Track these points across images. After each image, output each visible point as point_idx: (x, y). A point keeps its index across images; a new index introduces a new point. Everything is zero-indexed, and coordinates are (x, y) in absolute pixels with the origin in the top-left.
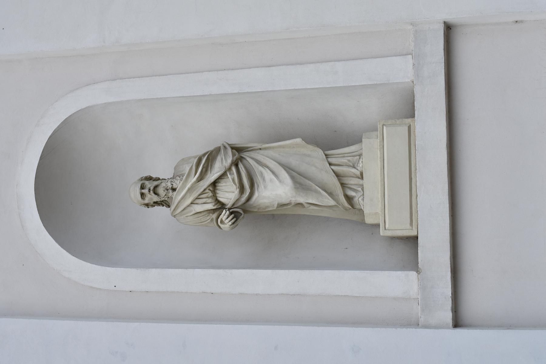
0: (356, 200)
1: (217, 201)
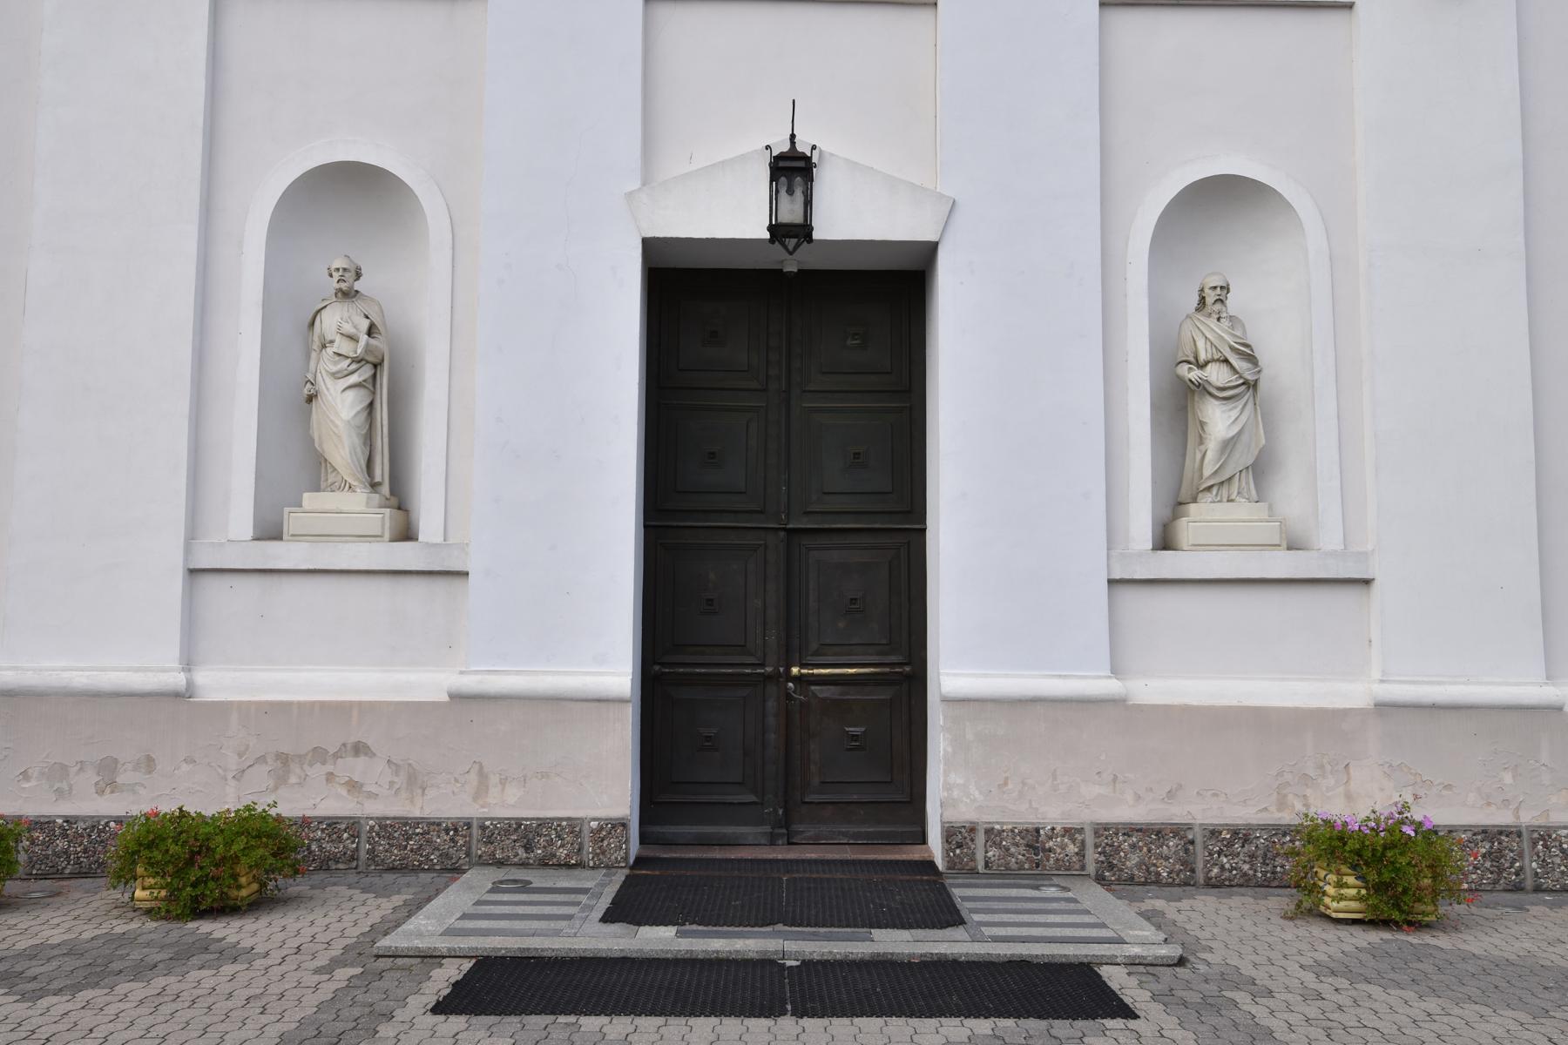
0: (1209, 495)
1: (1207, 363)
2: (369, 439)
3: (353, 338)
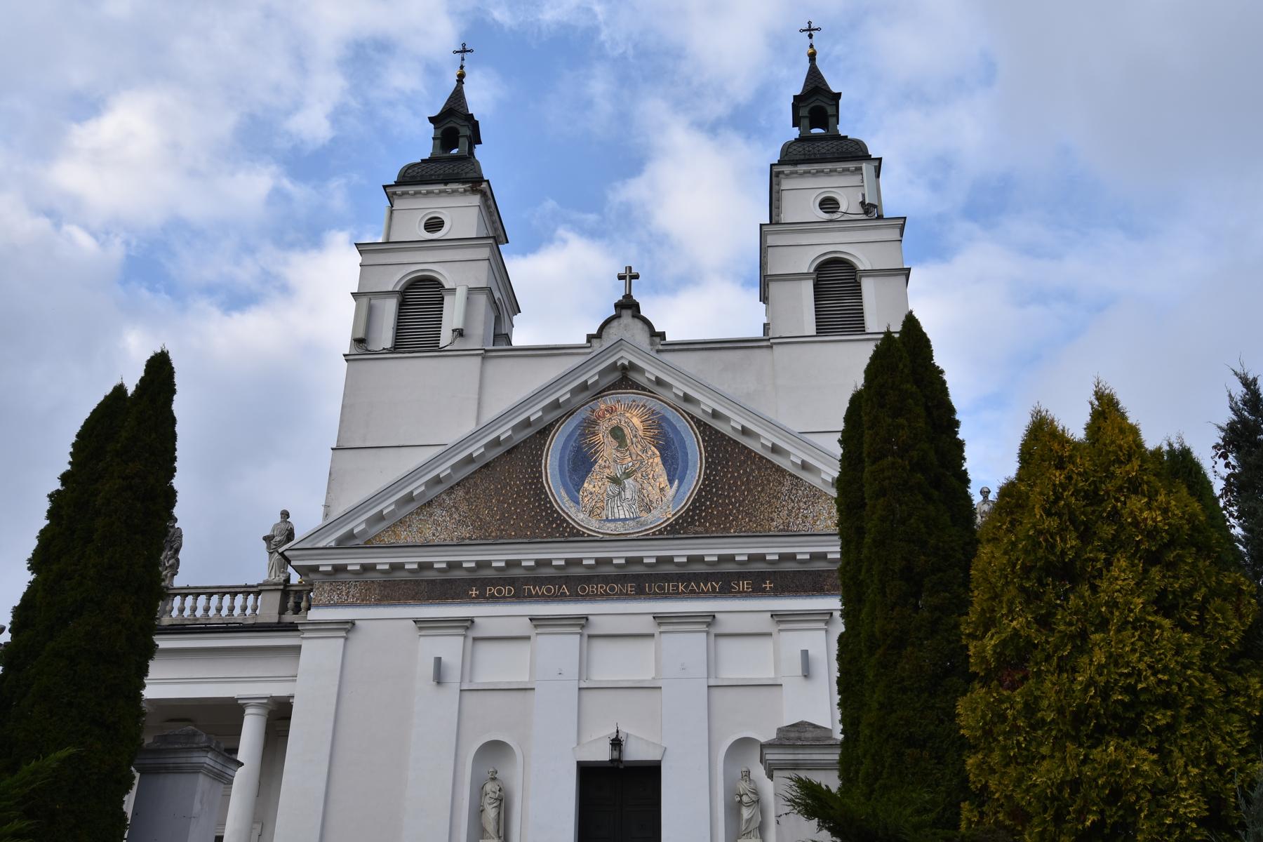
2: (498, 823)
3: (495, 792)
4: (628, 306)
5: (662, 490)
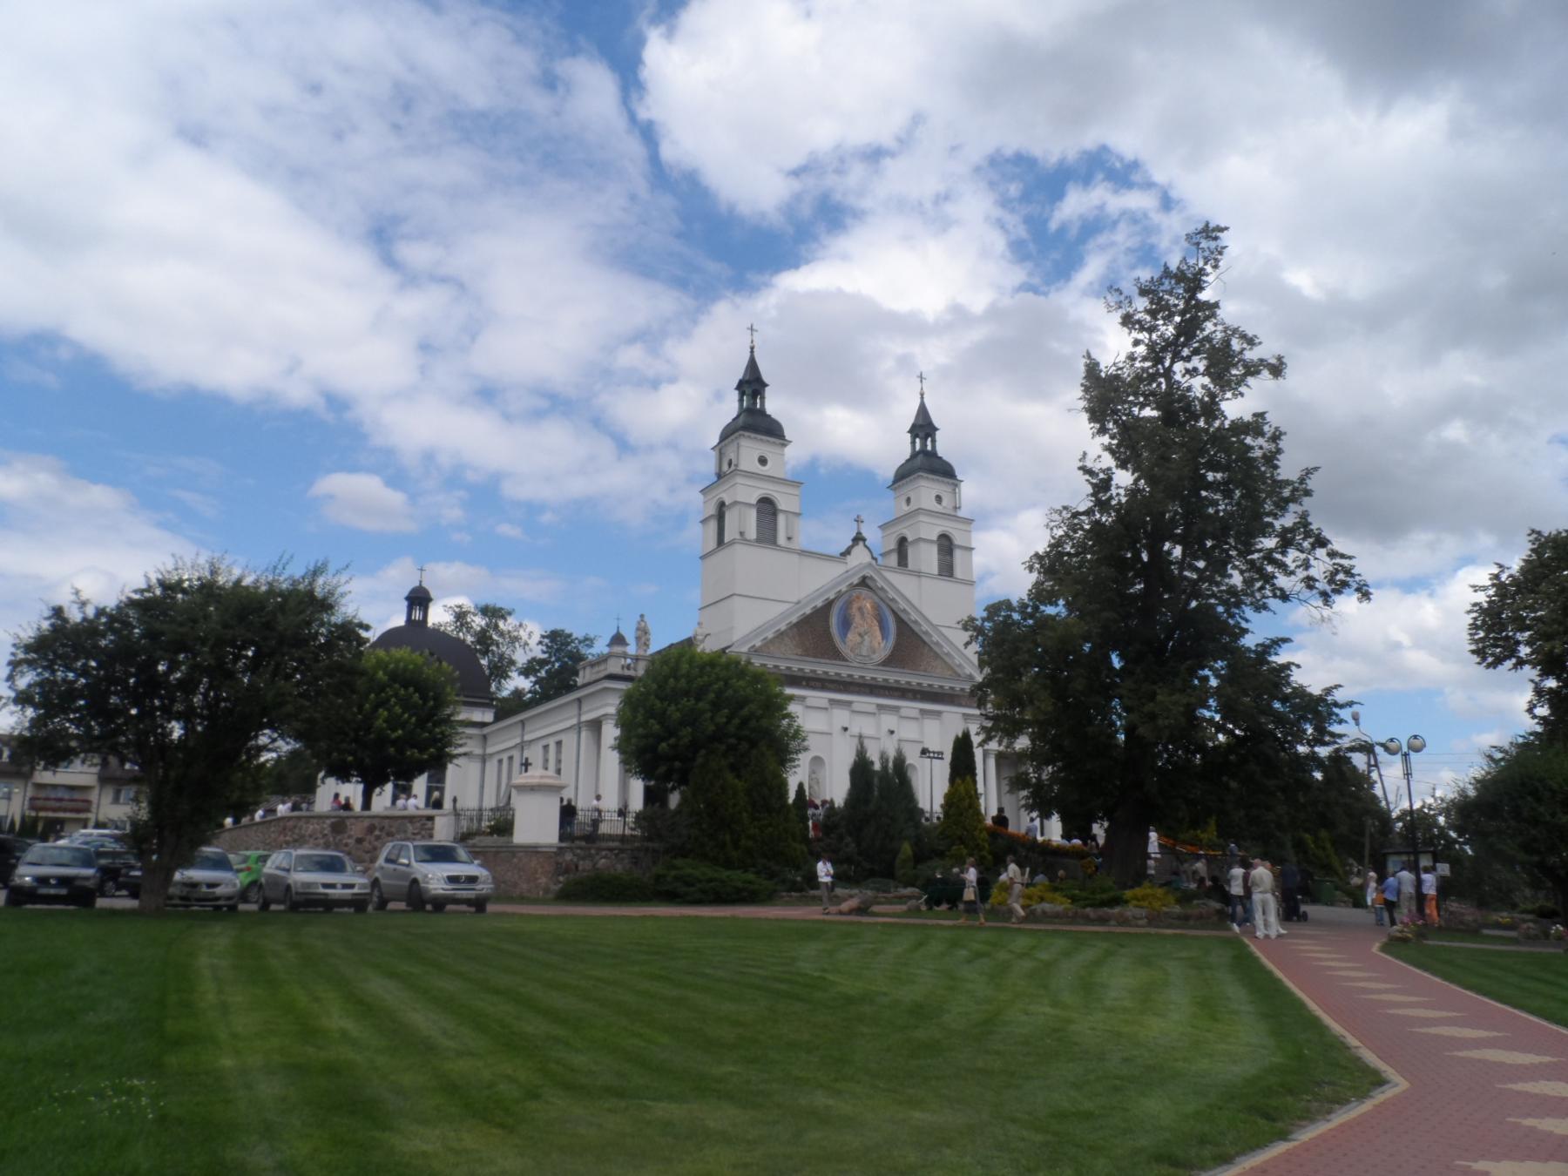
4: (859, 539)
5: (879, 643)
